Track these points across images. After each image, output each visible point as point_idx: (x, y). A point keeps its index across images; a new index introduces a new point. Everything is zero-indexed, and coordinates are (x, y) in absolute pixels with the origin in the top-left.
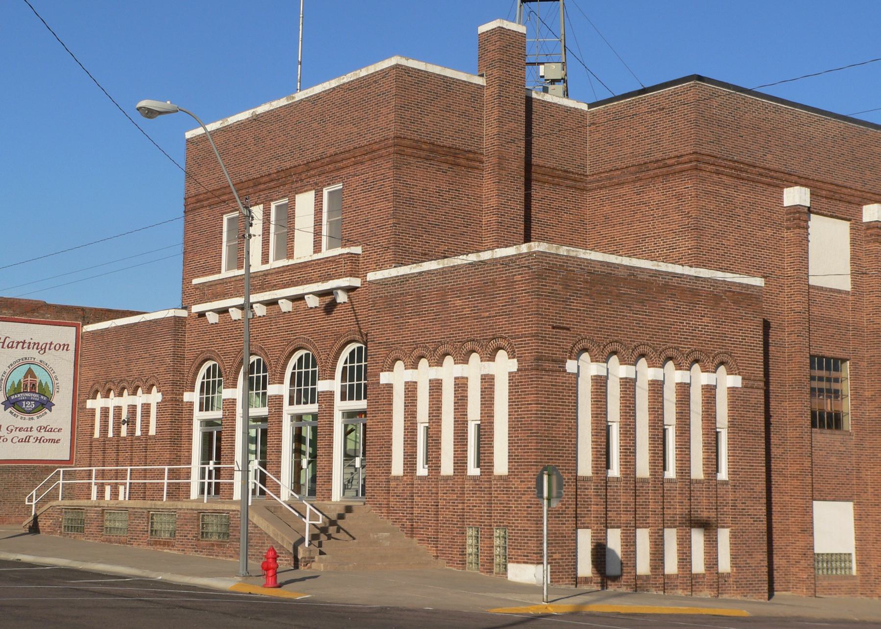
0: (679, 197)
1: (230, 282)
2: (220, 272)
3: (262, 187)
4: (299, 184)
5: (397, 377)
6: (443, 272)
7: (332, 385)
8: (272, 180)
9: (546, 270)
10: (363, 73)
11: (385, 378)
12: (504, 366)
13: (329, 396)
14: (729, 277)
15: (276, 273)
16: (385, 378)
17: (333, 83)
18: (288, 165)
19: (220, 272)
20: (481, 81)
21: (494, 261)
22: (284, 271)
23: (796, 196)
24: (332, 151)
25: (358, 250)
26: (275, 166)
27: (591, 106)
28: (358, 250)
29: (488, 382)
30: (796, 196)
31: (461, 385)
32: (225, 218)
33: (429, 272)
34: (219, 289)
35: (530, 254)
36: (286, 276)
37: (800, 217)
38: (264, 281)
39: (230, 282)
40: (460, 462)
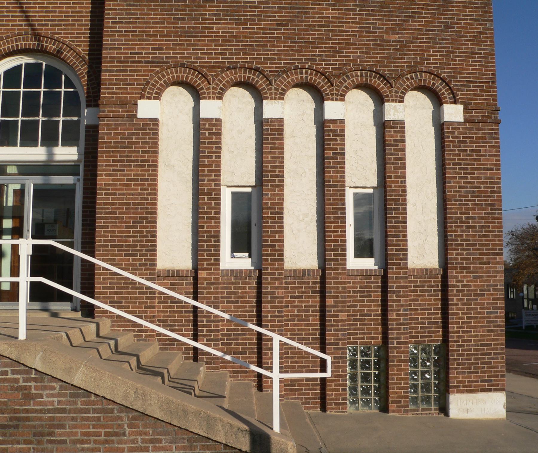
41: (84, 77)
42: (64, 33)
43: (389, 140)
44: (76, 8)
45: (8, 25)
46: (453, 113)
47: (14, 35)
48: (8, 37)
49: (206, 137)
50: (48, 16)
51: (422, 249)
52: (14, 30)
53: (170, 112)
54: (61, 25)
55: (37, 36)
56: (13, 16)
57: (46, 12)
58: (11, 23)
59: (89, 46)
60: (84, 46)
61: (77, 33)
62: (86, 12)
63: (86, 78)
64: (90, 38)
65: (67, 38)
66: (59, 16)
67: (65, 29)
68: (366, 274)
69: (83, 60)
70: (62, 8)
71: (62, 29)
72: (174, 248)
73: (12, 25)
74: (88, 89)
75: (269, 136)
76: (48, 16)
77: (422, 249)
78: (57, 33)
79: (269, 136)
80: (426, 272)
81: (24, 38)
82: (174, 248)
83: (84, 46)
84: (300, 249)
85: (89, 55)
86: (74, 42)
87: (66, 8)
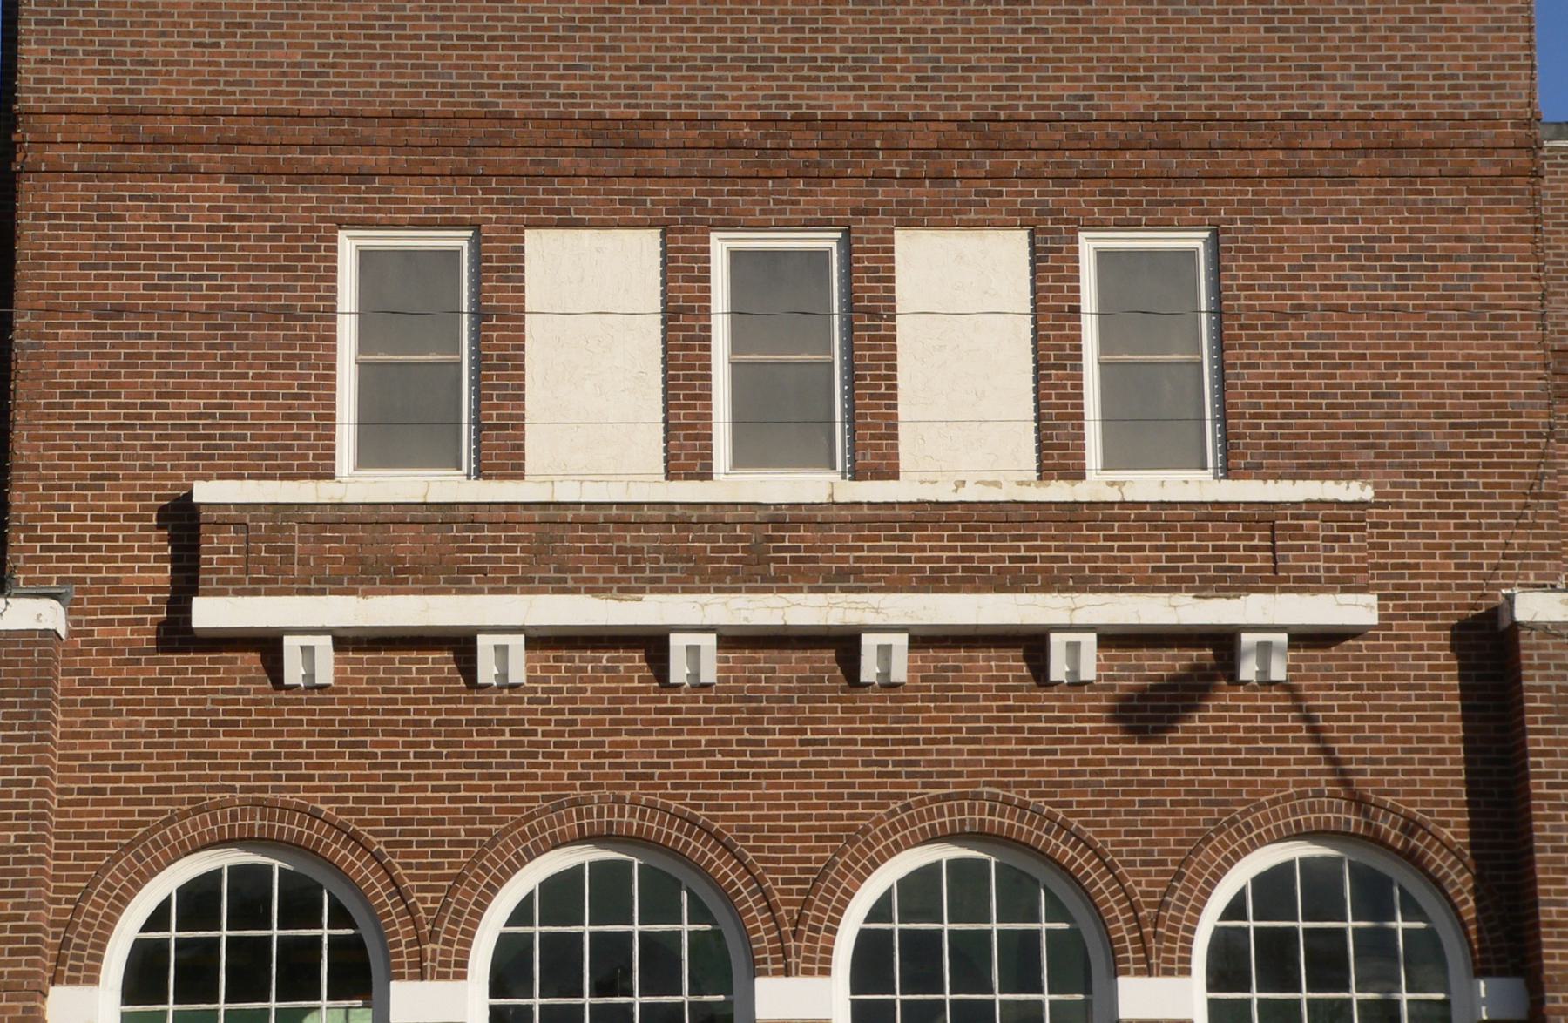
1: (507, 524)
3: (650, 161)
4: (925, 192)
8: (733, 146)
15: (859, 522)
19: (324, 471)
22: (918, 524)
24: (1137, 101)
26: (741, 98)
32: (348, 246)
34: (407, 544)
36: (935, 548)
38: (765, 547)
39: (507, 524)
41: (1465, 902)
42: (1407, 793)
44: (1425, 729)
45: (1270, 773)
47: (1288, 798)
48: (1274, 802)
50: (1363, 751)
52: (1286, 784)
54: (1395, 773)
55: (1359, 802)
56: (1279, 751)
57: (1357, 740)
58: (1276, 768)
59: (1470, 824)
60: (1458, 825)
61: (1437, 793)
62: (1452, 740)
63: (1472, 904)
64: (1468, 803)
65: (1413, 804)
66: (1388, 751)
67: (1407, 783)
69: (1460, 858)
70: (1393, 729)
71: (1398, 783)
73: (1281, 773)
74: (1479, 930)
76: (1363, 751)
78: (1388, 793)
81: (1312, 805)
83: (1458, 825)
85: (1472, 846)
86: (1430, 813)
87: (1403, 729)
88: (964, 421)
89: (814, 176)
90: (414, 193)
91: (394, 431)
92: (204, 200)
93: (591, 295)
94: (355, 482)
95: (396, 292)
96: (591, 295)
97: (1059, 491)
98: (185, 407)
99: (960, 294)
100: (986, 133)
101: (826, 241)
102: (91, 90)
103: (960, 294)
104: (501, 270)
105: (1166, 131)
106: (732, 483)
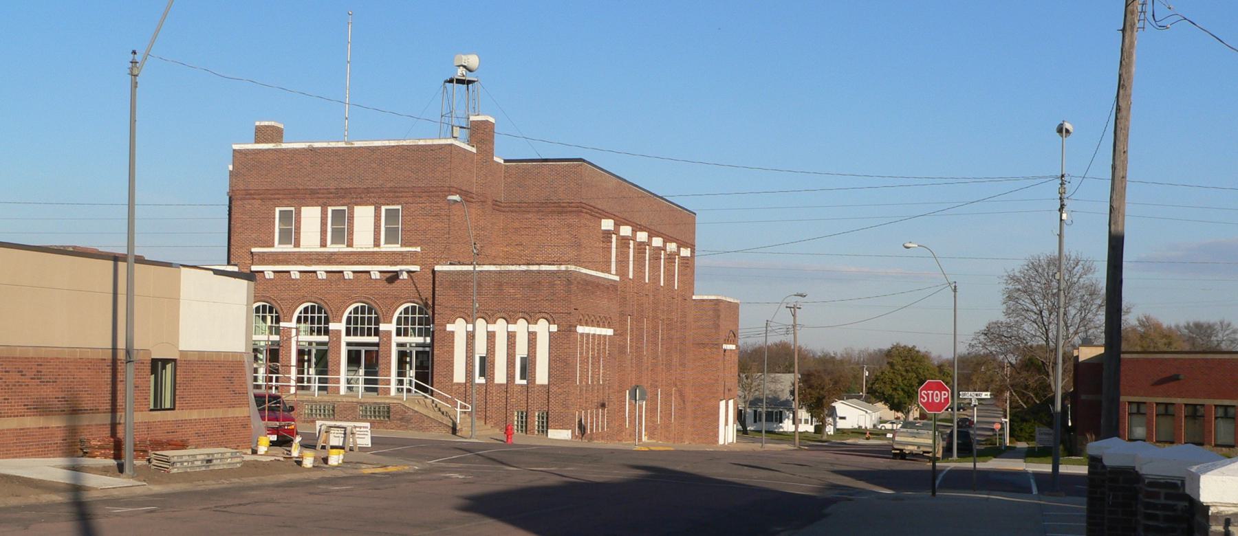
0: (569, 226)
2: (273, 246)
5: (459, 328)
6: (500, 272)
7: (389, 327)
9: (568, 277)
10: (422, 142)
11: (449, 327)
12: (543, 329)
13: (389, 333)
14: (584, 271)
16: (449, 327)
17: (393, 143)
18: (348, 186)
19: (273, 246)
20: (474, 150)
21: (539, 272)
23: (607, 224)
25: (418, 249)
26: (332, 185)
27: (506, 161)
28: (418, 249)
29: (532, 338)
30: (607, 224)
31: (511, 337)
32: (277, 210)
33: (490, 272)
35: (567, 271)
37: (608, 234)
40: (510, 376)
43: (532, 338)
46: (554, 328)
49: (471, 337)
51: (542, 377)
53: (459, 328)
68: (522, 386)
72: (459, 376)
75: (491, 336)
77: (542, 377)
79: (491, 336)
80: (542, 386)
82: (459, 376)
84: (500, 377)
88: (363, 239)
89: (343, 197)
90: (286, 202)
91: (285, 237)
92: (257, 203)
93: (311, 216)
94: (278, 248)
95: (285, 216)
96: (311, 216)
97: (376, 249)
98: (254, 236)
99: (364, 216)
100: (368, 191)
101: (345, 208)
102: (242, 187)
103: (364, 216)
104: (299, 214)
105: (394, 190)
106: (331, 248)
